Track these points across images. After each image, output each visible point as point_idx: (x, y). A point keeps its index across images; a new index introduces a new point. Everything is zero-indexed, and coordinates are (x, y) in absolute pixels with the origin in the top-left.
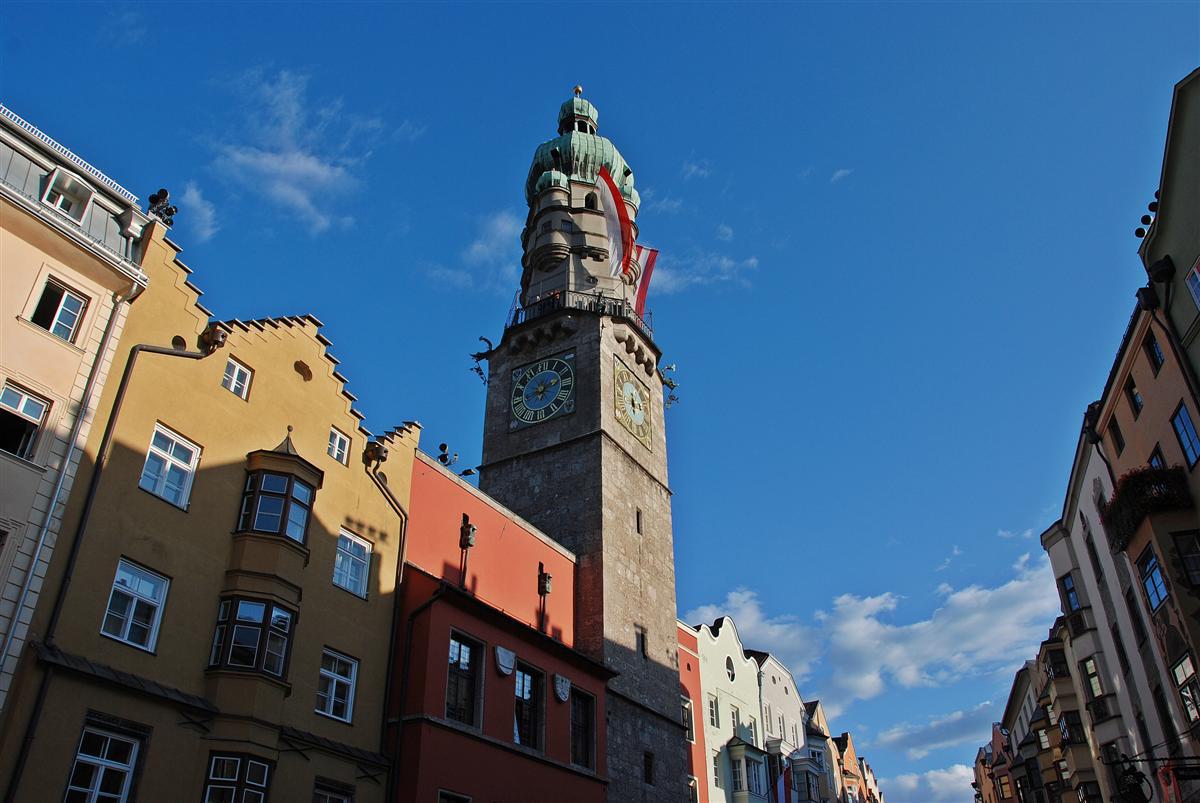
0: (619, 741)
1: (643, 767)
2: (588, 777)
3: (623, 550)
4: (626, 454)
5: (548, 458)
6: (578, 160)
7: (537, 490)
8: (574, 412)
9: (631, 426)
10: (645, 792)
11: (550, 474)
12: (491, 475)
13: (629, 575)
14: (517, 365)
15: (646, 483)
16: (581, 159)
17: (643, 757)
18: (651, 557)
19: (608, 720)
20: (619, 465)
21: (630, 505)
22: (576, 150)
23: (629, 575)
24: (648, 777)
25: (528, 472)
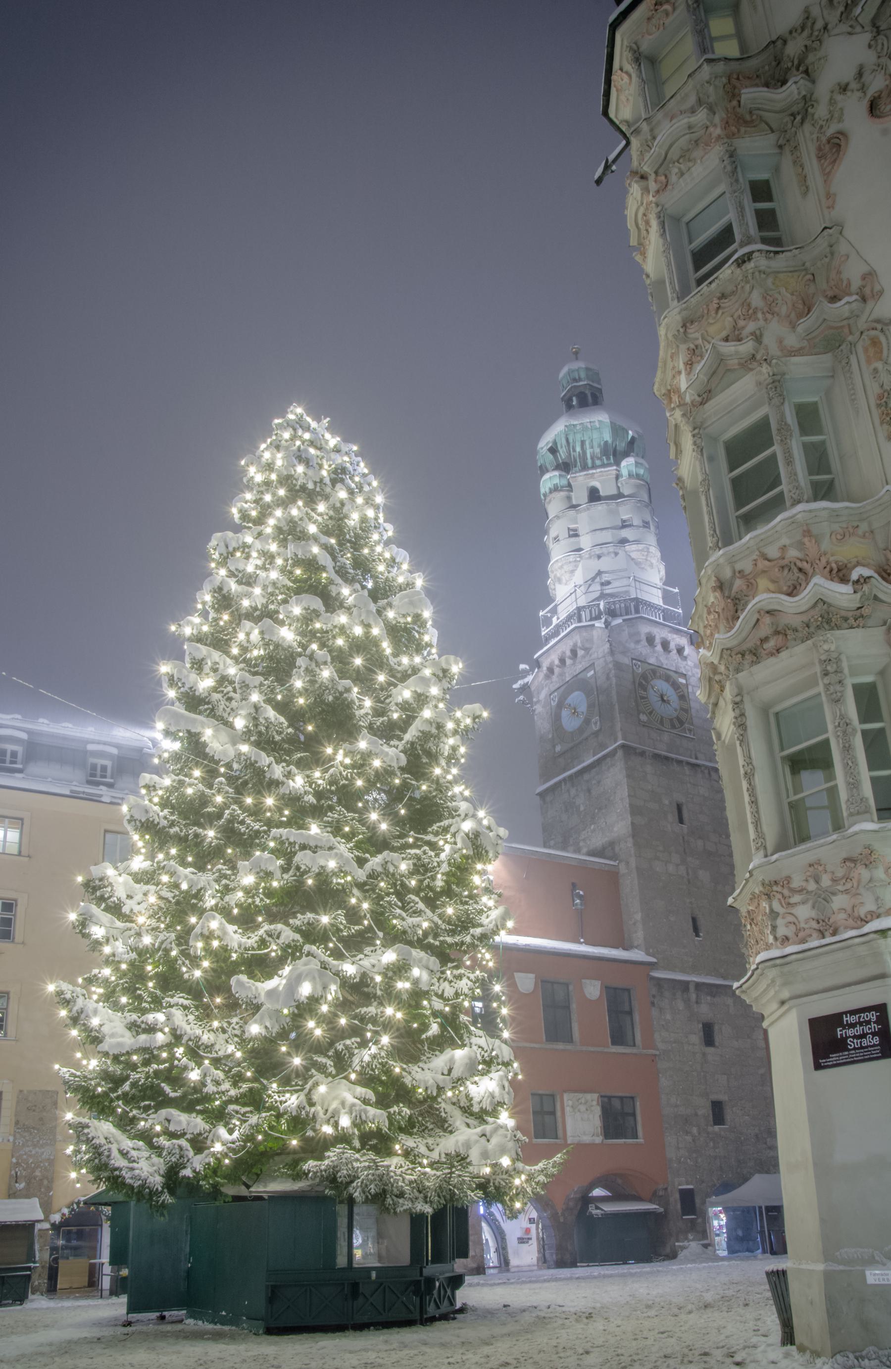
0: (668, 1017)
1: (702, 1034)
2: (635, 1054)
3: (661, 848)
4: (656, 757)
5: (586, 776)
6: (574, 451)
7: (582, 808)
8: (600, 730)
9: (662, 723)
10: (704, 1054)
11: (589, 791)
12: (548, 799)
13: (671, 868)
14: (553, 689)
15: (688, 772)
16: (578, 449)
17: (701, 1026)
18: (700, 843)
19: (653, 1004)
20: (649, 769)
21: (667, 802)
22: (571, 441)
23: (671, 868)
24: (709, 1039)
25: (573, 792)
